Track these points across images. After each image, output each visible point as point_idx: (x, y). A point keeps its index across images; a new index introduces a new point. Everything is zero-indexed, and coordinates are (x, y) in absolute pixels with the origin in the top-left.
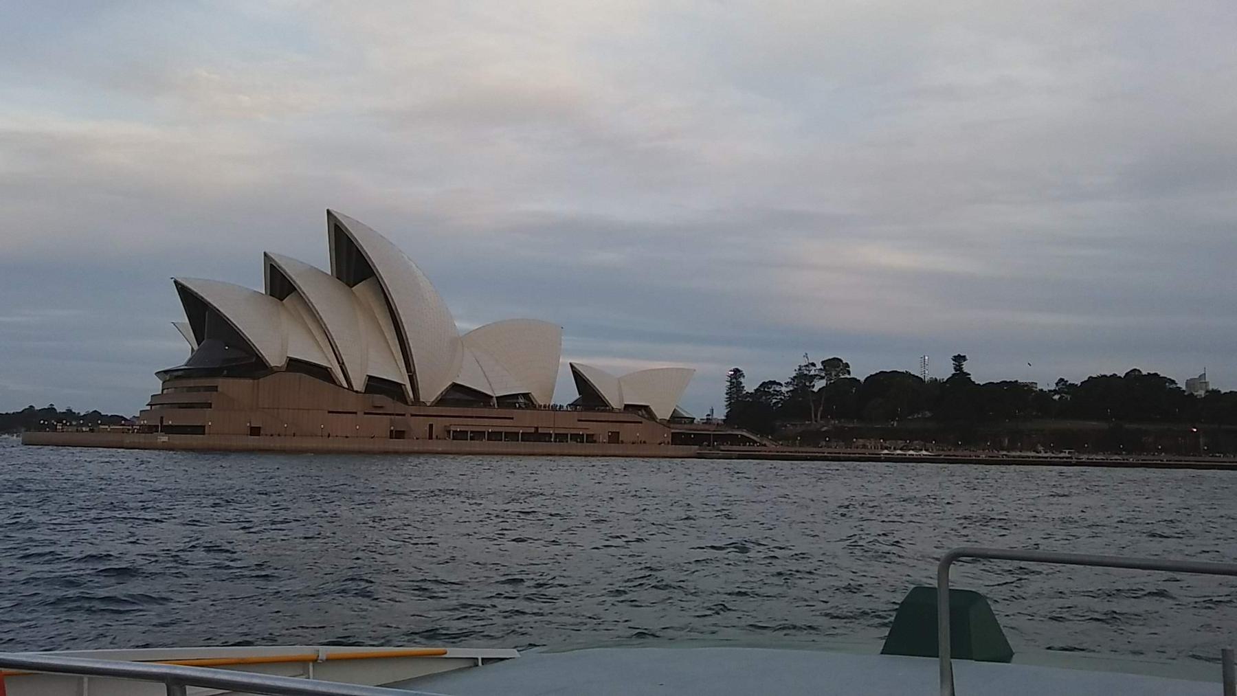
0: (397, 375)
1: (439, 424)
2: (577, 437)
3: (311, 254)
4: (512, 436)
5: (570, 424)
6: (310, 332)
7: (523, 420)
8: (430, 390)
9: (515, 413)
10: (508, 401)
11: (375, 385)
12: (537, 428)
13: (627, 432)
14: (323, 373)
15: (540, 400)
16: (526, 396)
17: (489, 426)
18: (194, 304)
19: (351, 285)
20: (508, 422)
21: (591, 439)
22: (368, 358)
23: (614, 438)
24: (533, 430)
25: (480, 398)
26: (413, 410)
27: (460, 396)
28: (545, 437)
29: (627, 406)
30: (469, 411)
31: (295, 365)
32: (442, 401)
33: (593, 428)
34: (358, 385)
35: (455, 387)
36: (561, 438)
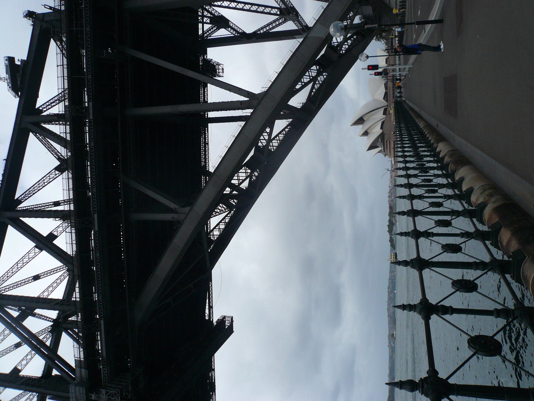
0: (382, 110)
3: (360, 129)
8: (385, 103)
10: (386, 88)
11: (384, 113)
14: (383, 123)
31: (381, 128)
32: (387, 101)
34: (385, 116)
35: (384, 99)
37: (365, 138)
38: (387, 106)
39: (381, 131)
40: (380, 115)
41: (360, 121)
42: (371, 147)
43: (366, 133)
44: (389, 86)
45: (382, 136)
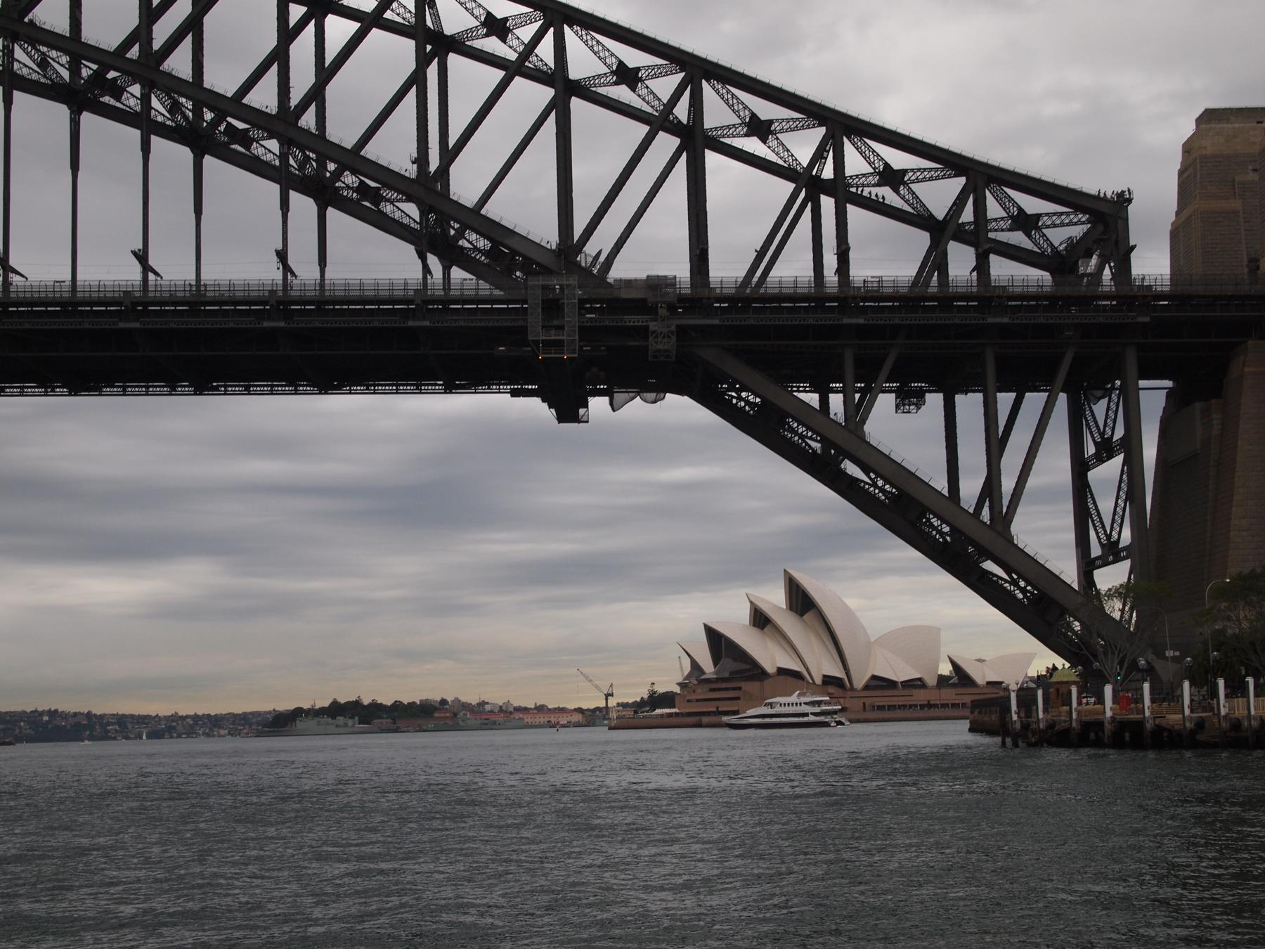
0: (837, 672)
1: (868, 701)
3: (775, 598)
5: (949, 695)
7: (920, 696)
8: (860, 681)
10: (909, 684)
11: (828, 680)
15: (931, 681)
16: (920, 679)
25: (891, 684)
26: (849, 694)
27: (879, 684)
28: (936, 706)
29: (988, 683)
31: (781, 671)
34: (818, 681)
35: (874, 677)
36: (944, 706)
37: (745, 615)
38: (852, 688)
39: (770, 669)
40: (822, 664)
41: (801, 601)
42: (715, 639)
43: (760, 620)
44: (915, 692)
45: (750, 670)
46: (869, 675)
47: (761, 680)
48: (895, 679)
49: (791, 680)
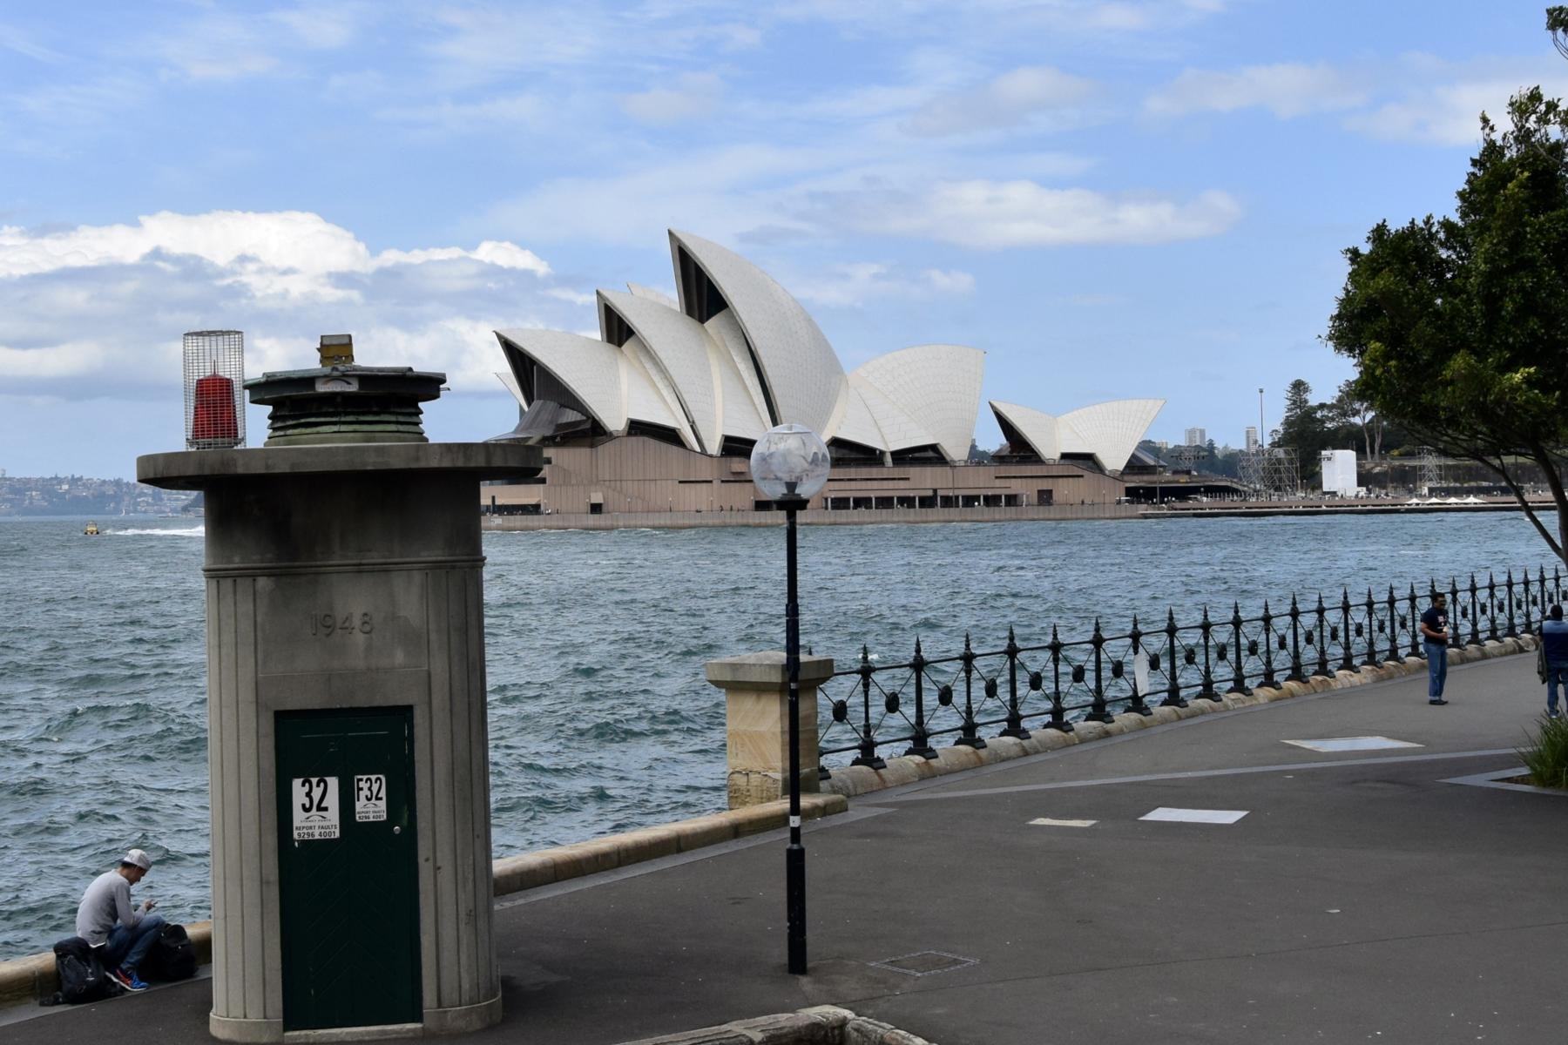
2: (991, 501)
4: (907, 502)
5: (983, 481)
6: (654, 385)
9: (913, 472)
12: (935, 491)
13: (1064, 491)
14: (669, 436)
17: (874, 490)
18: (522, 362)
19: (702, 320)
20: (902, 484)
21: (1012, 500)
22: (722, 410)
23: (1045, 497)
24: (930, 493)
30: (852, 472)
33: (1015, 487)
34: (714, 447)
39: (615, 422)
46: (826, 437)
47: (592, 446)
48: (883, 448)
49: (652, 443)
